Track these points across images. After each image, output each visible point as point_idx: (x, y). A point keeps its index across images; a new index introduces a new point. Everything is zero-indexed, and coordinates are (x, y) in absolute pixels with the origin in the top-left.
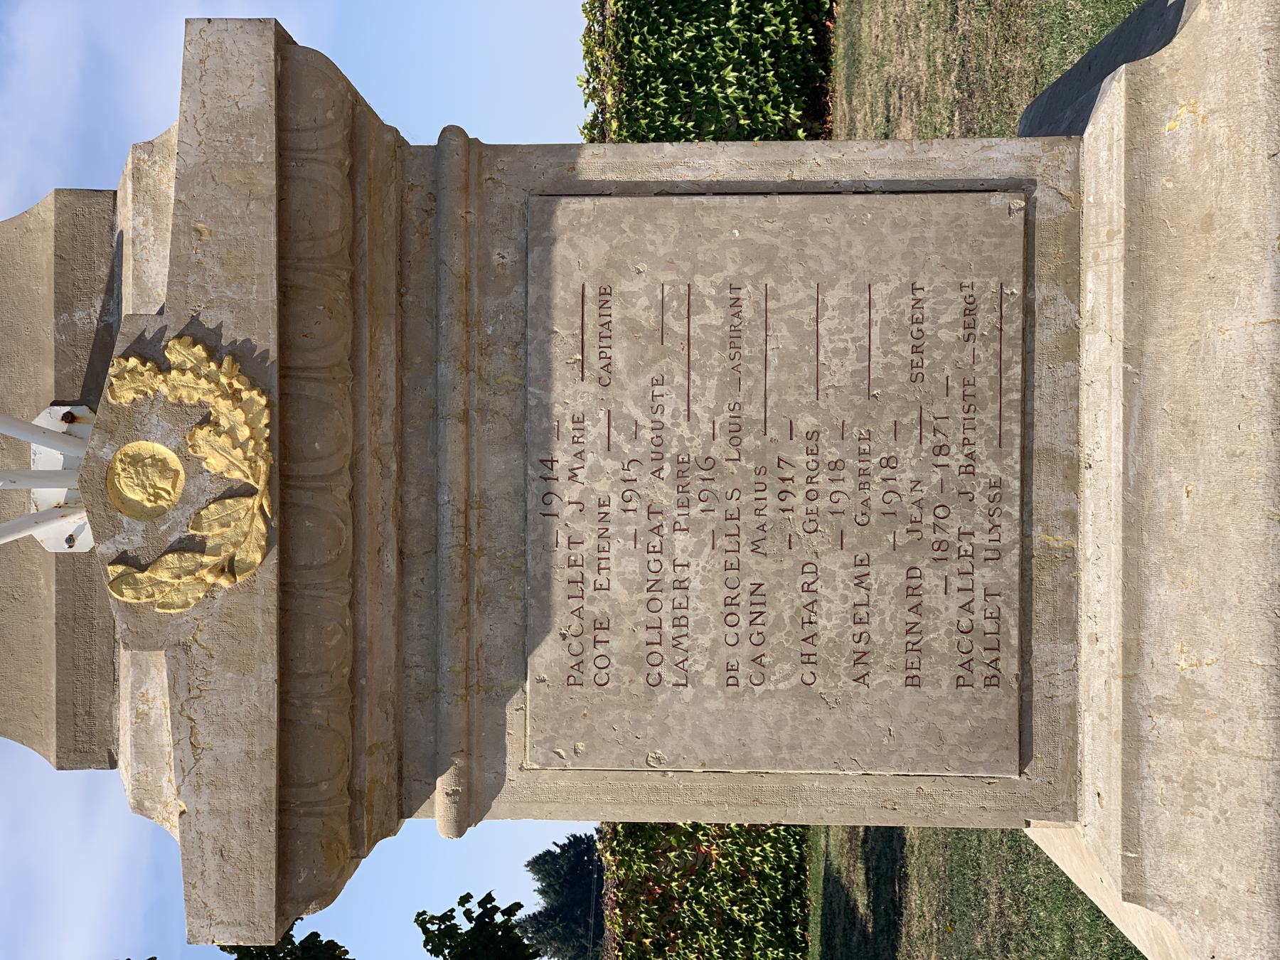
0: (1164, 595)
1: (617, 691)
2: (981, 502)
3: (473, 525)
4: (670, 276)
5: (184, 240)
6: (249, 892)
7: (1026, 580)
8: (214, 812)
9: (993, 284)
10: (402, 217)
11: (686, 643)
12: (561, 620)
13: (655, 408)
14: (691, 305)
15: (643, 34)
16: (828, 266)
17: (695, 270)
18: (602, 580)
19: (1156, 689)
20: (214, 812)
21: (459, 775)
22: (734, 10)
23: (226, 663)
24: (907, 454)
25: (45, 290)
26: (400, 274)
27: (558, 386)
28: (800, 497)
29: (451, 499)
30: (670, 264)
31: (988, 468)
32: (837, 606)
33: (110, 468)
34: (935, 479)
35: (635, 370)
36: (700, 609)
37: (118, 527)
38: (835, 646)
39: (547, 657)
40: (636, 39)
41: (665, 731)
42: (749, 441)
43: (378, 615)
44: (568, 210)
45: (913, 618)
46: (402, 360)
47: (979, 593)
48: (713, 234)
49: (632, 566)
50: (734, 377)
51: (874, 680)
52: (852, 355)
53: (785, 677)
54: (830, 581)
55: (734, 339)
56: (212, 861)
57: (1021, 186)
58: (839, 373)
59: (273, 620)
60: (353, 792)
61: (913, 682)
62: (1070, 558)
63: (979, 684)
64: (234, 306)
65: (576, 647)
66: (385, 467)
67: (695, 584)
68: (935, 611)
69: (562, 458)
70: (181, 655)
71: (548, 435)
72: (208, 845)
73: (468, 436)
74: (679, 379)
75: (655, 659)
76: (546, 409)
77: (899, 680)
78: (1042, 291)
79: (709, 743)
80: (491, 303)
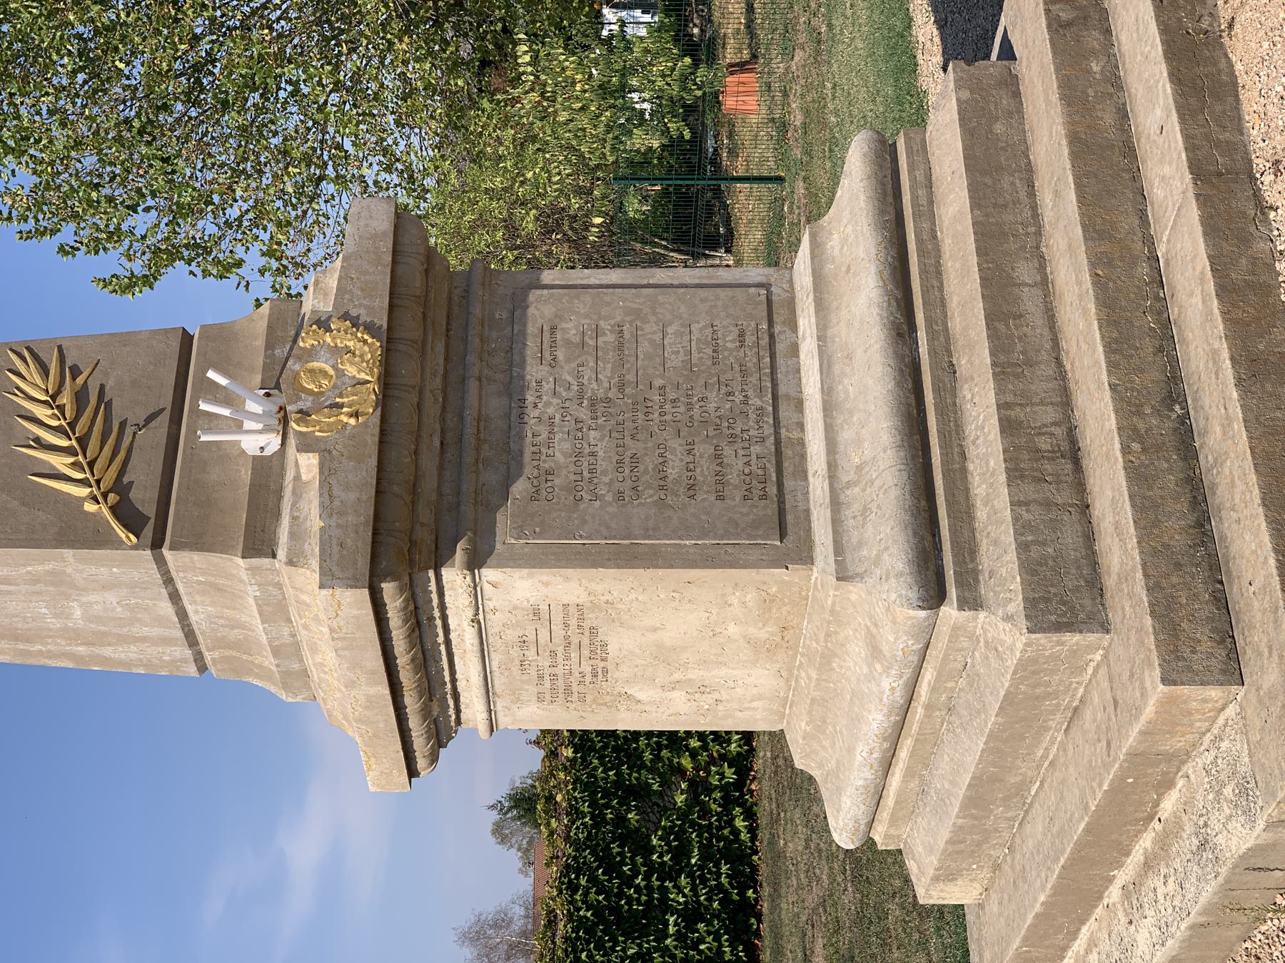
0: (845, 435)
1: (558, 503)
2: (753, 416)
3: (482, 428)
4: (587, 321)
5: (344, 282)
6: (355, 563)
7: (778, 453)
8: (338, 526)
9: (753, 324)
10: (450, 299)
11: (596, 481)
12: (528, 470)
13: (579, 376)
14: (598, 332)
15: (589, 951)
16: (668, 317)
17: (600, 318)
18: (551, 452)
19: (844, 478)
20: (338, 526)
21: (470, 540)
22: (671, 930)
23: (349, 458)
24: (712, 396)
25: (260, 343)
26: (448, 324)
27: (528, 368)
28: (656, 415)
29: (470, 415)
30: (587, 316)
31: (755, 401)
32: (677, 463)
33: (298, 373)
34: (728, 406)
35: (568, 360)
36: (602, 465)
37: (299, 398)
38: (677, 482)
39: (519, 488)
40: (584, 956)
41: (584, 522)
42: (628, 391)
43: (429, 463)
44: (534, 295)
45: (719, 468)
46: (447, 359)
47: (754, 457)
48: (609, 304)
49: (567, 446)
50: (621, 362)
51: (699, 498)
52: (682, 353)
53: (650, 496)
54: (673, 452)
55: (620, 347)
56: (336, 549)
57: (766, 286)
58: (675, 361)
59: (377, 439)
60: (412, 543)
61: (721, 498)
62: (802, 443)
63: (756, 499)
64: (366, 307)
65: (535, 483)
66: (436, 400)
67: (601, 454)
68: (731, 466)
69: (530, 398)
70: (327, 455)
71: (524, 388)
72: (334, 541)
73: (480, 389)
74: (592, 364)
75: (579, 488)
76: (522, 377)
77: (712, 497)
78: (777, 329)
79: (608, 527)
80: (494, 334)
